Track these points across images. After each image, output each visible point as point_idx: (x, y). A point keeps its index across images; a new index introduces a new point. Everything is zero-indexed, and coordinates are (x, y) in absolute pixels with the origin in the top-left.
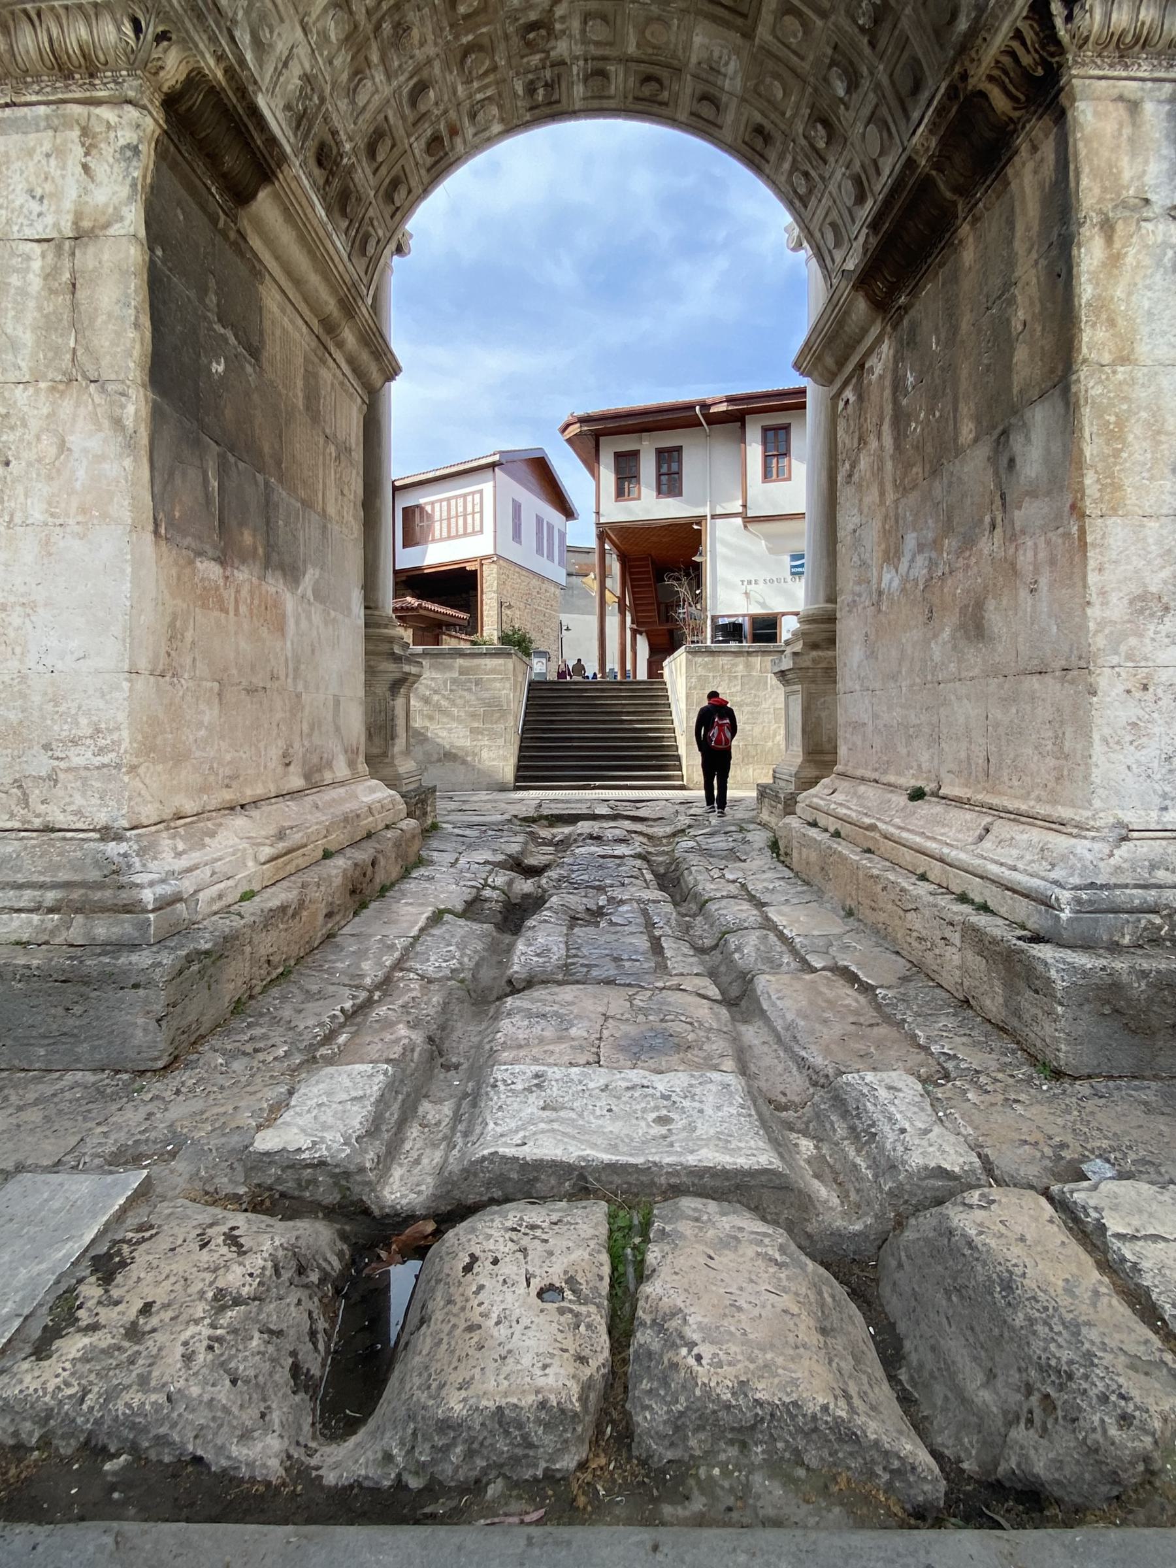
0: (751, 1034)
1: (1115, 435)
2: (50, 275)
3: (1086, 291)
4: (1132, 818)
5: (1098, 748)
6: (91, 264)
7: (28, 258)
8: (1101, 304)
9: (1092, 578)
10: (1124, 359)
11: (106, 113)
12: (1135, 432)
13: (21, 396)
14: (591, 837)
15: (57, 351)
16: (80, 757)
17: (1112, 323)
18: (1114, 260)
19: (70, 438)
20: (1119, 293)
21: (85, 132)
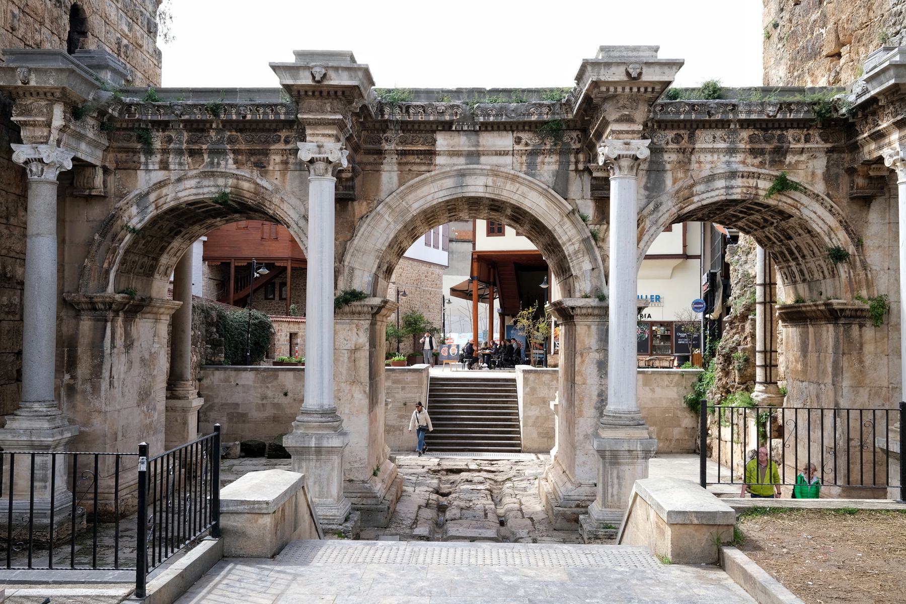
0: (502, 528)
1: (581, 400)
2: (349, 358)
3: (577, 369)
4: (582, 482)
5: (576, 467)
6: (359, 356)
7: (344, 354)
8: (580, 371)
9: (576, 431)
10: (584, 384)
11: (362, 322)
12: (586, 400)
13: (343, 385)
14: (467, 481)
15: (351, 375)
16: (356, 465)
17: (582, 375)
18: (583, 362)
19: (354, 395)
20: (584, 369)
21: (357, 326)
